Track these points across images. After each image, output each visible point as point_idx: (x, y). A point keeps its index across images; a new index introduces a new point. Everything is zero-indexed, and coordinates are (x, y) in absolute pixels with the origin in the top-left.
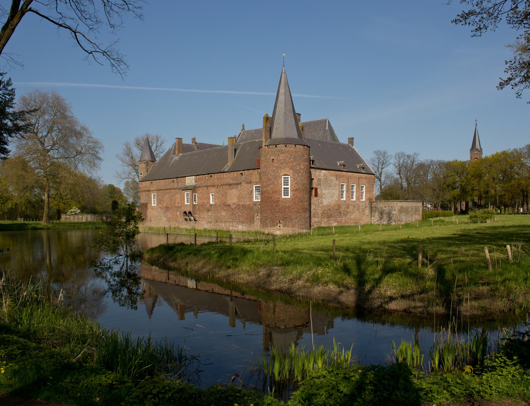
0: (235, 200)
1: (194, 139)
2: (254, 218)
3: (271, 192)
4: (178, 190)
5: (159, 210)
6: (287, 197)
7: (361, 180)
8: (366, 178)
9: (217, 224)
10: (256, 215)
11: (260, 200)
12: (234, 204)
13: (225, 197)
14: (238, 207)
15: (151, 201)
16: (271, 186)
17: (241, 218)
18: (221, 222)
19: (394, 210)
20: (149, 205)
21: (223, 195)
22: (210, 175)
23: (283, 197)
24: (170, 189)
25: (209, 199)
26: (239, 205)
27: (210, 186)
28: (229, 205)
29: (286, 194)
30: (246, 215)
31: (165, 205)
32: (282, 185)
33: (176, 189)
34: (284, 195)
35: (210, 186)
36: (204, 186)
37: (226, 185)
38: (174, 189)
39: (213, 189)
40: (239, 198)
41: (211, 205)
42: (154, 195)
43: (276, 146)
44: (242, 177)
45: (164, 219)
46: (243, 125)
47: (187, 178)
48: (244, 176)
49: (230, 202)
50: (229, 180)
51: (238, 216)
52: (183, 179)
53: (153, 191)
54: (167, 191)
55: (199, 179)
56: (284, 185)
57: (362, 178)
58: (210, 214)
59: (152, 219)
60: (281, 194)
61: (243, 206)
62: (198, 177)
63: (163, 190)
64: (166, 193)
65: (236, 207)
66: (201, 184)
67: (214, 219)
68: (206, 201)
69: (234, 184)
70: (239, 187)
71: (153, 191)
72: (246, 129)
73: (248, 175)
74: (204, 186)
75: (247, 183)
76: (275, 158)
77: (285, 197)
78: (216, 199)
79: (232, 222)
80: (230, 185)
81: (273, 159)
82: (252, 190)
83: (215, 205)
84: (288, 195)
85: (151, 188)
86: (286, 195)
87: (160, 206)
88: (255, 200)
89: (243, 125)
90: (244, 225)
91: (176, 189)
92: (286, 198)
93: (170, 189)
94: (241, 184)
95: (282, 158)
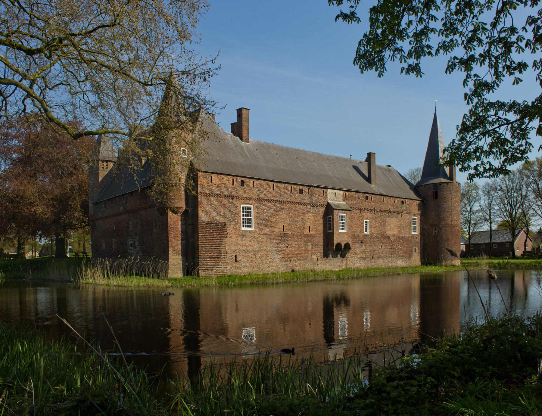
0: (395, 232)
2: (412, 252)
4: (309, 207)
5: (263, 239)
9: (373, 260)
10: (414, 249)
12: (394, 235)
14: (399, 239)
17: (400, 252)
18: (379, 257)
20: (230, 228)
22: (366, 195)
26: (399, 237)
27: (365, 209)
28: (388, 237)
30: (405, 249)
31: (278, 229)
33: (306, 204)
35: (365, 209)
36: (358, 209)
39: (369, 215)
44: (404, 205)
47: (329, 190)
48: (404, 205)
49: (389, 233)
52: (321, 190)
55: (349, 197)
58: (364, 247)
59: (239, 258)
62: (347, 193)
63: (276, 201)
64: (281, 209)
66: (353, 204)
67: (370, 254)
68: (359, 230)
69: (395, 212)
74: (358, 209)
75: (407, 213)
78: (373, 229)
79: (391, 257)
80: (389, 212)
83: (371, 235)
87: (267, 231)
90: (403, 259)
91: (306, 204)
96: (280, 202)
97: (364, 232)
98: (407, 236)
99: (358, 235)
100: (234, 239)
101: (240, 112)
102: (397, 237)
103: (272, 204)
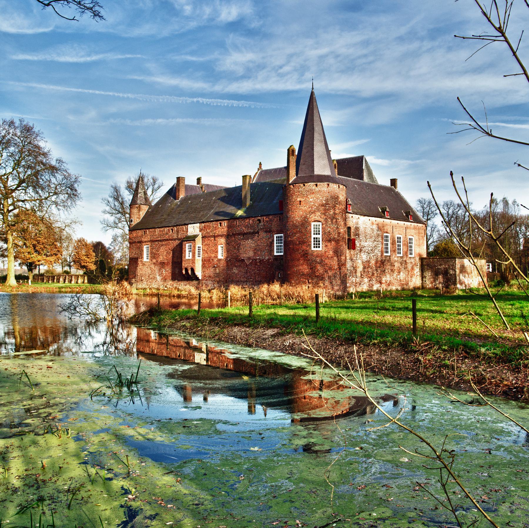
0: (251, 254)
1: (199, 180)
3: (298, 243)
5: (153, 266)
6: (318, 249)
7: (408, 231)
8: (415, 228)
11: (282, 254)
12: (249, 258)
13: (238, 250)
14: (254, 262)
15: (142, 254)
16: (298, 235)
17: (257, 277)
19: (452, 269)
20: (139, 260)
21: (235, 247)
23: (313, 249)
24: (167, 240)
25: (217, 252)
27: (218, 236)
28: (243, 260)
29: (317, 245)
30: (265, 273)
32: (311, 234)
34: (314, 247)
35: (218, 236)
37: (239, 234)
38: (171, 240)
40: (255, 250)
41: (220, 260)
42: (147, 248)
43: (304, 185)
45: (159, 278)
46: (260, 164)
47: (189, 226)
48: (262, 224)
49: (244, 256)
50: (244, 228)
51: (255, 273)
53: (146, 242)
54: (164, 243)
55: (204, 227)
56: (314, 234)
57: (410, 228)
60: (310, 245)
61: (260, 262)
63: (159, 241)
64: (162, 245)
65: (251, 263)
66: (208, 233)
68: (213, 255)
70: (256, 237)
71: (146, 242)
72: (264, 168)
73: (267, 222)
74: (211, 236)
75: (266, 232)
76: (302, 200)
77: (315, 249)
80: (244, 234)
81: (300, 201)
82: (273, 241)
84: (319, 247)
85: (143, 239)
86: (317, 247)
87: (154, 261)
88: (276, 254)
89: (260, 164)
92: (316, 251)
93: (167, 240)
94: (258, 233)
95: (311, 200)
96: (161, 241)
97: (217, 257)
98: (267, 258)
99: (213, 260)
100: (141, 267)
101: (178, 179)
102: (253, 260)
103: (157, 243)
